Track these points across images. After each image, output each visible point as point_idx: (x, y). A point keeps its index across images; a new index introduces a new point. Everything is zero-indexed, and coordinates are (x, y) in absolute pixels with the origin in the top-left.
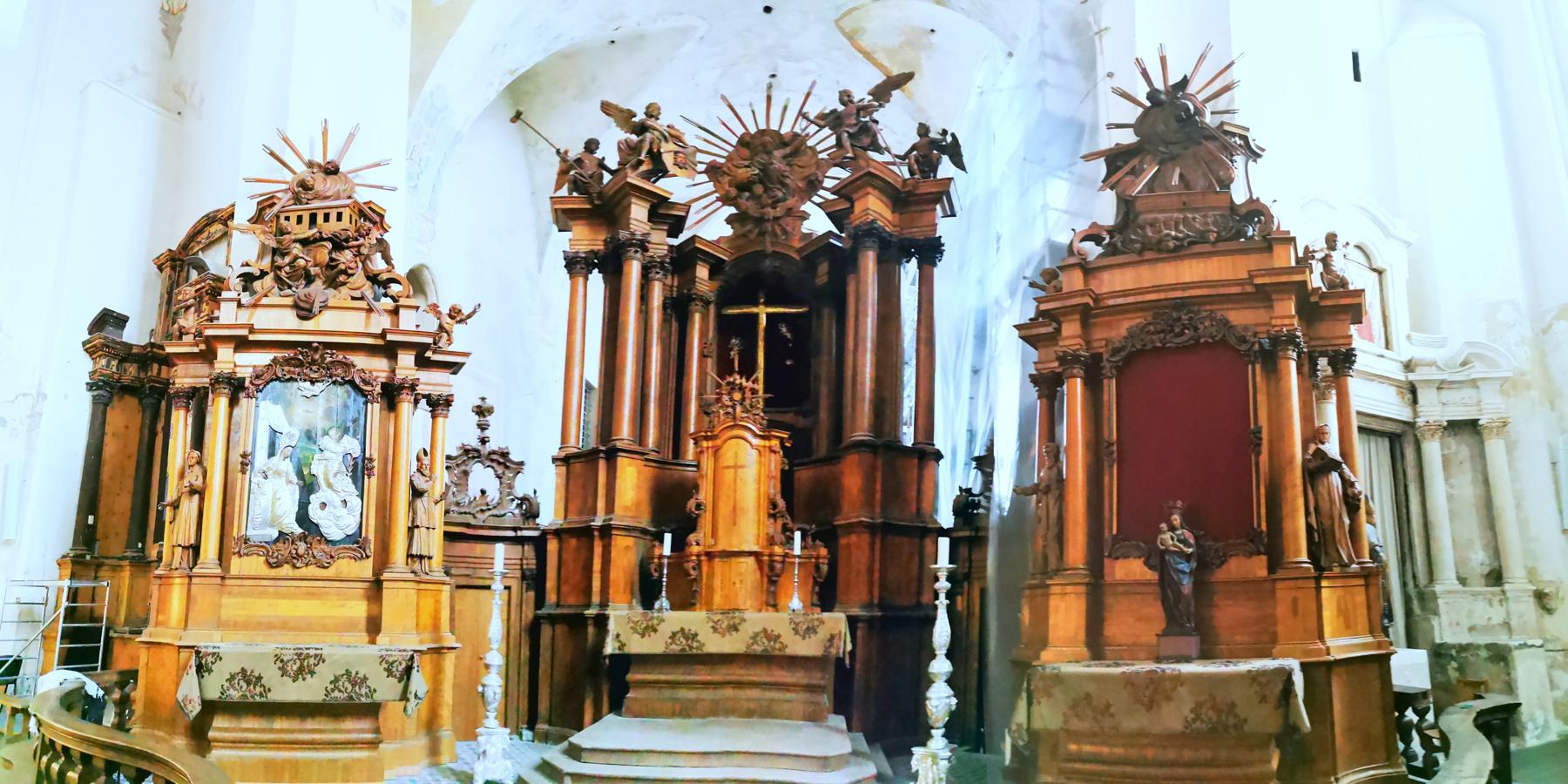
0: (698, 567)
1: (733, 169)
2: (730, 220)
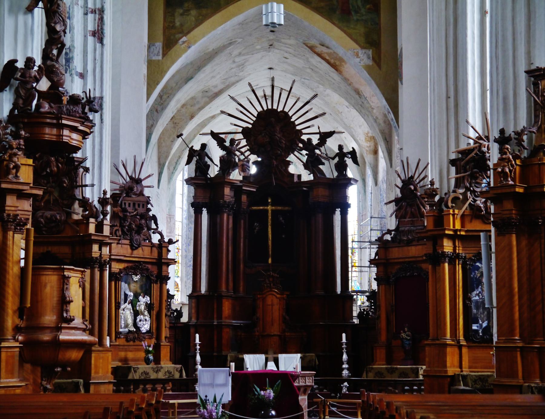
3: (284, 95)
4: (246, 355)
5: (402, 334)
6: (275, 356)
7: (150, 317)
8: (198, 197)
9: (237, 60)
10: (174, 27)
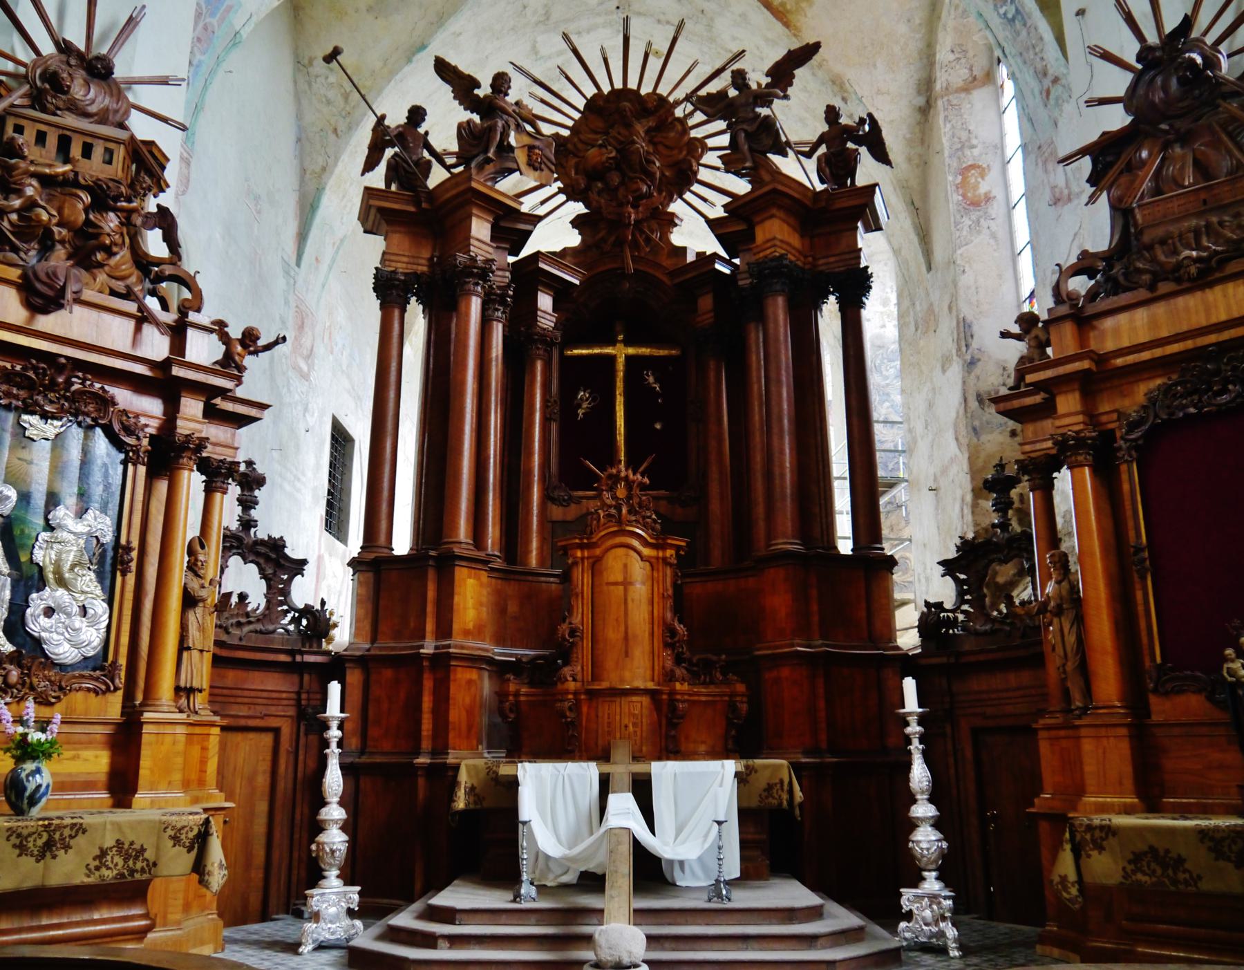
0: (576, 707)
1: (580, 146)
2: (577, 223)
3: (654, 64)
4: (527, 765)
5: (1231, 665)
6: (639, 768)
7: (110, 602)
8: (393, 258)
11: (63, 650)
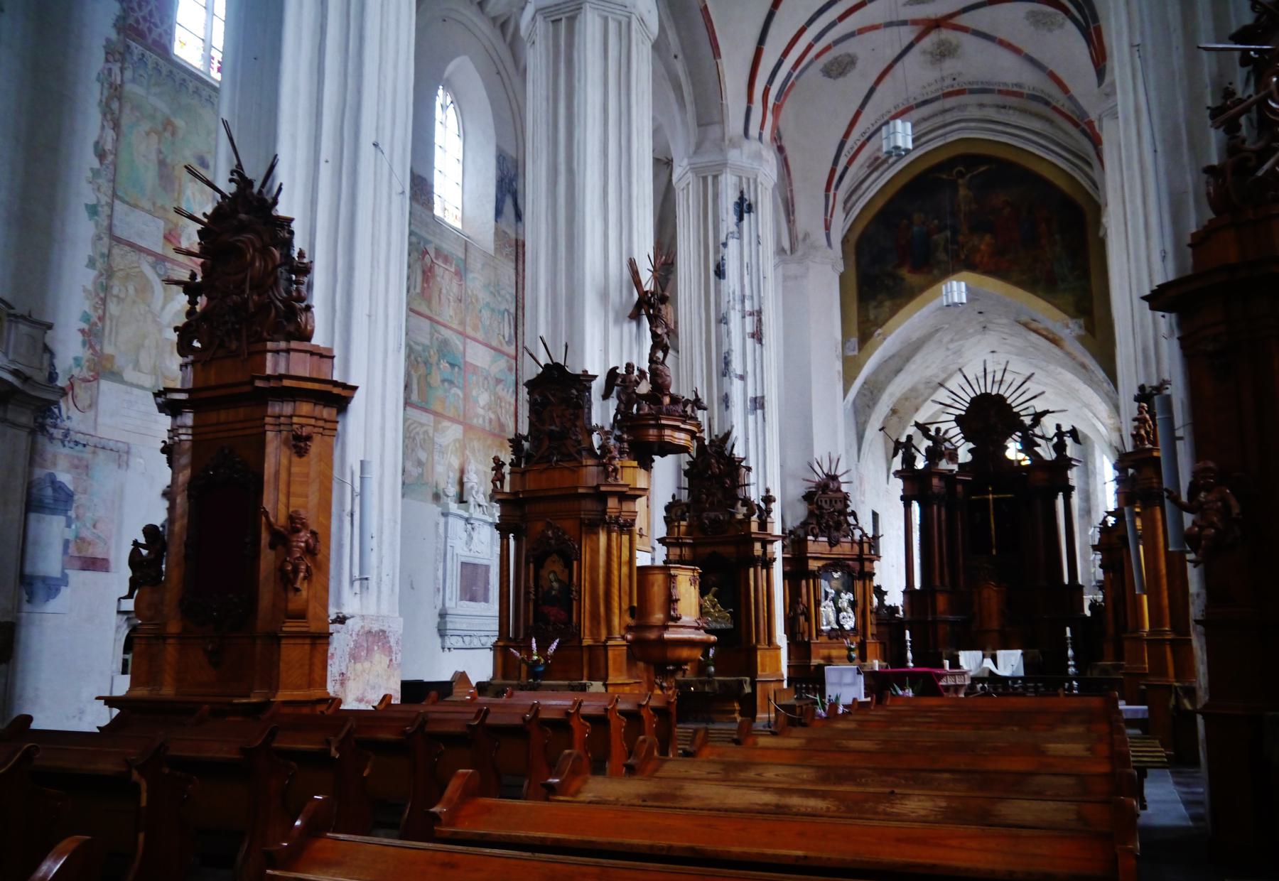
6: (993, 652)
9: (951, 346)
10: (868, 320)
11: (847, 627)
